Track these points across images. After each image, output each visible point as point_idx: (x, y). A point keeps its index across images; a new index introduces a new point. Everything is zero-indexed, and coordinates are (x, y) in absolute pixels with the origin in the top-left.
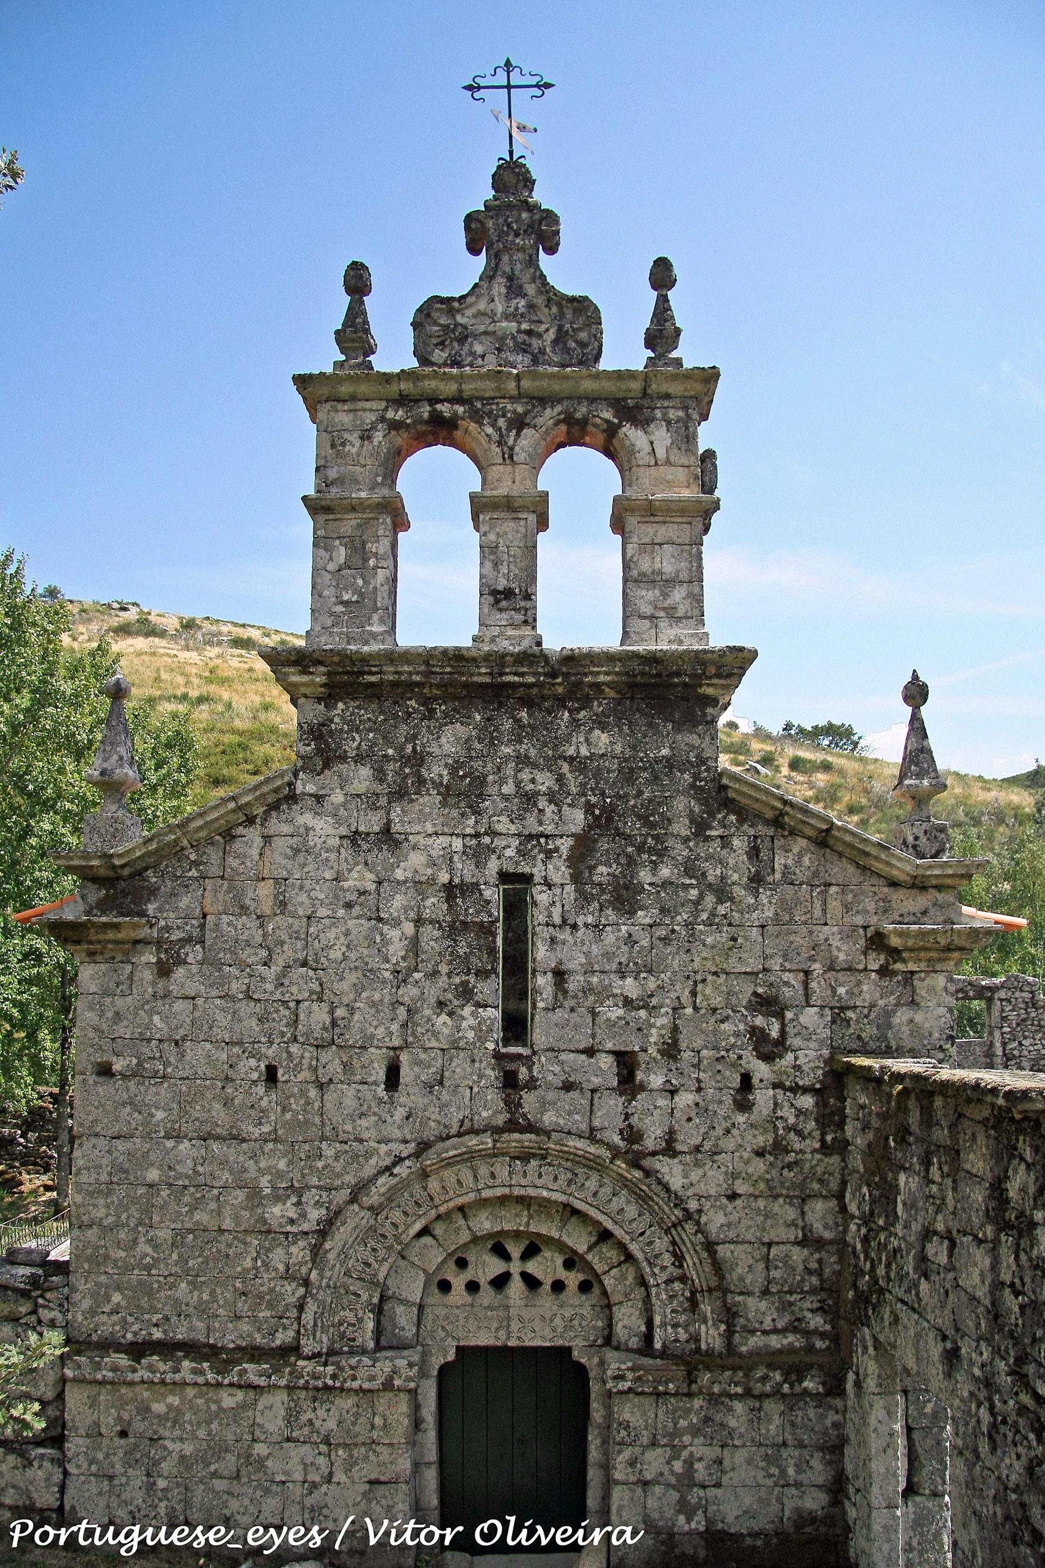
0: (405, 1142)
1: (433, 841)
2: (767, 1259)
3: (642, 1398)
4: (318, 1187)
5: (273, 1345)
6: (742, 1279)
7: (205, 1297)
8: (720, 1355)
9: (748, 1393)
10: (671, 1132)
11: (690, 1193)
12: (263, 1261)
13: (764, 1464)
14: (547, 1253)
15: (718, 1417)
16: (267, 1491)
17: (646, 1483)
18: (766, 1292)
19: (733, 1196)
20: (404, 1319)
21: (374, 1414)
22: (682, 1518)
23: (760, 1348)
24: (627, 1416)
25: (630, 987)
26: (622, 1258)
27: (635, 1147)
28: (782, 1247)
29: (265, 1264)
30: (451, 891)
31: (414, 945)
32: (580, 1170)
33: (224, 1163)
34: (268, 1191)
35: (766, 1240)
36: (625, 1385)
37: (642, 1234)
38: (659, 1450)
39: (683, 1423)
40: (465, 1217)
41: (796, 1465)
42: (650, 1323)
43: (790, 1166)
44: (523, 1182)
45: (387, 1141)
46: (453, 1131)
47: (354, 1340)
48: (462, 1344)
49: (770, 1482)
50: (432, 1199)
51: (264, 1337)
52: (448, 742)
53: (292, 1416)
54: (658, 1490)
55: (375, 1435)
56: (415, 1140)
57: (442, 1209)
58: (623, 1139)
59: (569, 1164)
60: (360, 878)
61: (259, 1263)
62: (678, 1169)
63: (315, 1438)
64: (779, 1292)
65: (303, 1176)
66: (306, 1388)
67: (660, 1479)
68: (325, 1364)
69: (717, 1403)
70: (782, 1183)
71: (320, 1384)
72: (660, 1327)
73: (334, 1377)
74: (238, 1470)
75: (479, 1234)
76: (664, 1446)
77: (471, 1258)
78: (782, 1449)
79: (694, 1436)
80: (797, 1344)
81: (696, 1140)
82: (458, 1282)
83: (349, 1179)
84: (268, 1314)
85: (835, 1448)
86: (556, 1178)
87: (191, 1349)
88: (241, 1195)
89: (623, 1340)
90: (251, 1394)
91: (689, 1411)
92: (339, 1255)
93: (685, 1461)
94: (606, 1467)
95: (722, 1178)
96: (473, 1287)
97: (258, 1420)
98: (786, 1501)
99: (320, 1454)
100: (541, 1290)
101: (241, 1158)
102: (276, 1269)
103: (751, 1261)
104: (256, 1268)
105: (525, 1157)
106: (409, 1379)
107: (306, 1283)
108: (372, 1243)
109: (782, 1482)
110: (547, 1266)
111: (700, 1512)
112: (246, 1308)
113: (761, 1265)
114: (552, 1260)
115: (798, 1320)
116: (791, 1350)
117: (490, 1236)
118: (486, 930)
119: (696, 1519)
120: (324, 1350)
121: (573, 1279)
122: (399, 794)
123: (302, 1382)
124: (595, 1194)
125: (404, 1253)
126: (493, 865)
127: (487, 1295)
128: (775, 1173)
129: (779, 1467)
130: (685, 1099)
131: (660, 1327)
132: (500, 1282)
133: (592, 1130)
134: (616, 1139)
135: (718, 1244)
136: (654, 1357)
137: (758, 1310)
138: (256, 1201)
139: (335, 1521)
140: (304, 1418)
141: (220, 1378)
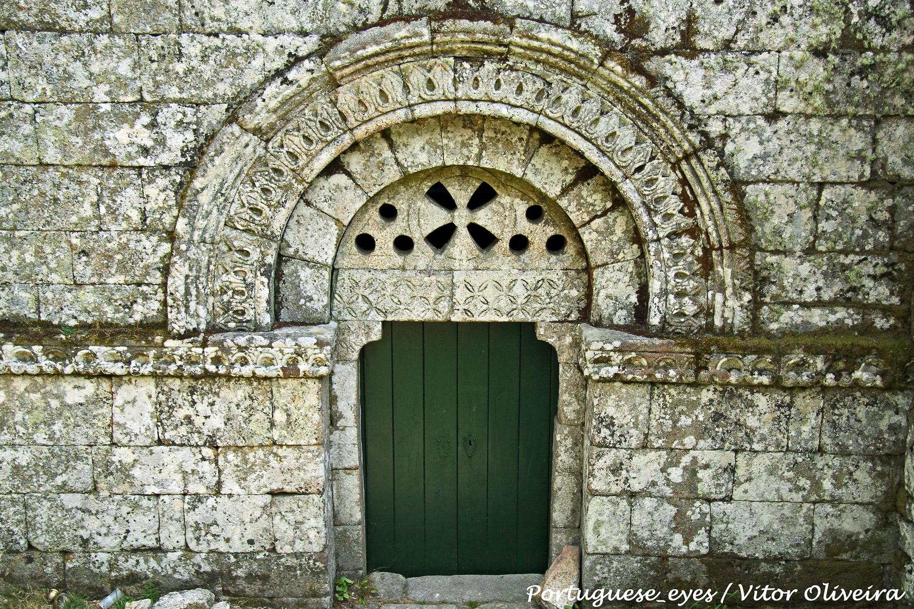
0: (303, 33)
2: (815, 206)
3: (631, 388)
4: (180, 102)
5: (131, 321)
6: (778, 232)
7: (29, 258)
8: (741, 333)
9: (777, 384)
10: (690, 20)
11: (712, 110)
12: (108, 207)
13: (791, 474)
14: (504, 199)
15: (732, 415)
16: (136, 506)
17: (633, 495)
18: (810, 251)
19: (774, 116)
20: (311, 285)
21: (274, 408)
22: (678, 539)
23: (797, 326)
24: (611, 410)
26: (609, 205)
27: (637, 42)
28: (840, 190)
29: (112, 212)
32: (553, 78)
33: (36, 67)
34: (108, 107)
35: (817, 179)
36: (609, 371)
37: (640, 169)
38: (652, 455)
39: (685, 421)
40: (392, 146)
41: (834, 476)
42: (643, 292)
43: (862, 72)
44: (474, 94)
45: (277, 33)
46: (373, 18)
47: (243, 313)
48: (390, 318)
49: (798, 497)
50: (344, 119)
51: (117, 311)
53: (163, 412)
54: (648, 503)
55: (276, 434)
56: (317, 31)
57: (360, 133)
58: (619, 30)
59: (540, 68)
61: (103, 210)
62: (697, 76)
63: (195, 438)
64: (829, 251)
65: (157, 85)
66: (179, 376)
67: (651, 489)
68: (204, 345)
69: (732, 395)
70: (849, 98)
71: (198, 370)
72: (659, 296)
73: (217, 361)
74: (95, 482)
75: (411, 171)
76: (659, 449)
77: (400, 205)
78: (817, 457)
79: (699, 437)
80: (849, 322)
81: (726, 33)
82: (385, 236)
83: (224, 88)
84: (121, 279)
85: (890, 458)
86: (520, 89)
88: (67, 113)
89: (606, 314)
90: (105, 385)
91: (693, 405)
92: (215, 198)
93: (685, 468)
94: (578, 475)
95: (759, 89)
96: (404, 244)
97: (117, 419)
98: (817, 521)
99: (203, 459)
100: (495, 248)
101: (62, 59)
102: (127, 218)
103: (792, 208)
104: (99, 218)
105: (477, 59)
106: (319, 363)
107: (171, 236)
108: (262, 181)
109: (814, 497)
110: (504, 216)
111: (702, 531)
112: (89, 271)
113: (807, 214)
114: (512, 208)
115: (853, 289)
116: (839, 329)
117: (426, 173)
119: (696, 539)
120: (203, 327)
121: (539, 234)
123: (173, 368)
124: (576, 112)
125: (309, 197)
127: (423, 254)
128: (838, 81)
129: (811, 478)
131: (659, 296)
132: (440, 238)
133: (575, 16)
134: (609, 30)
135: (747, 183)
136: (650, 336)
137: (798, 274)
138: (90, 123)
139: (228, 540)
140: (180, 414)
141: (59, 367)
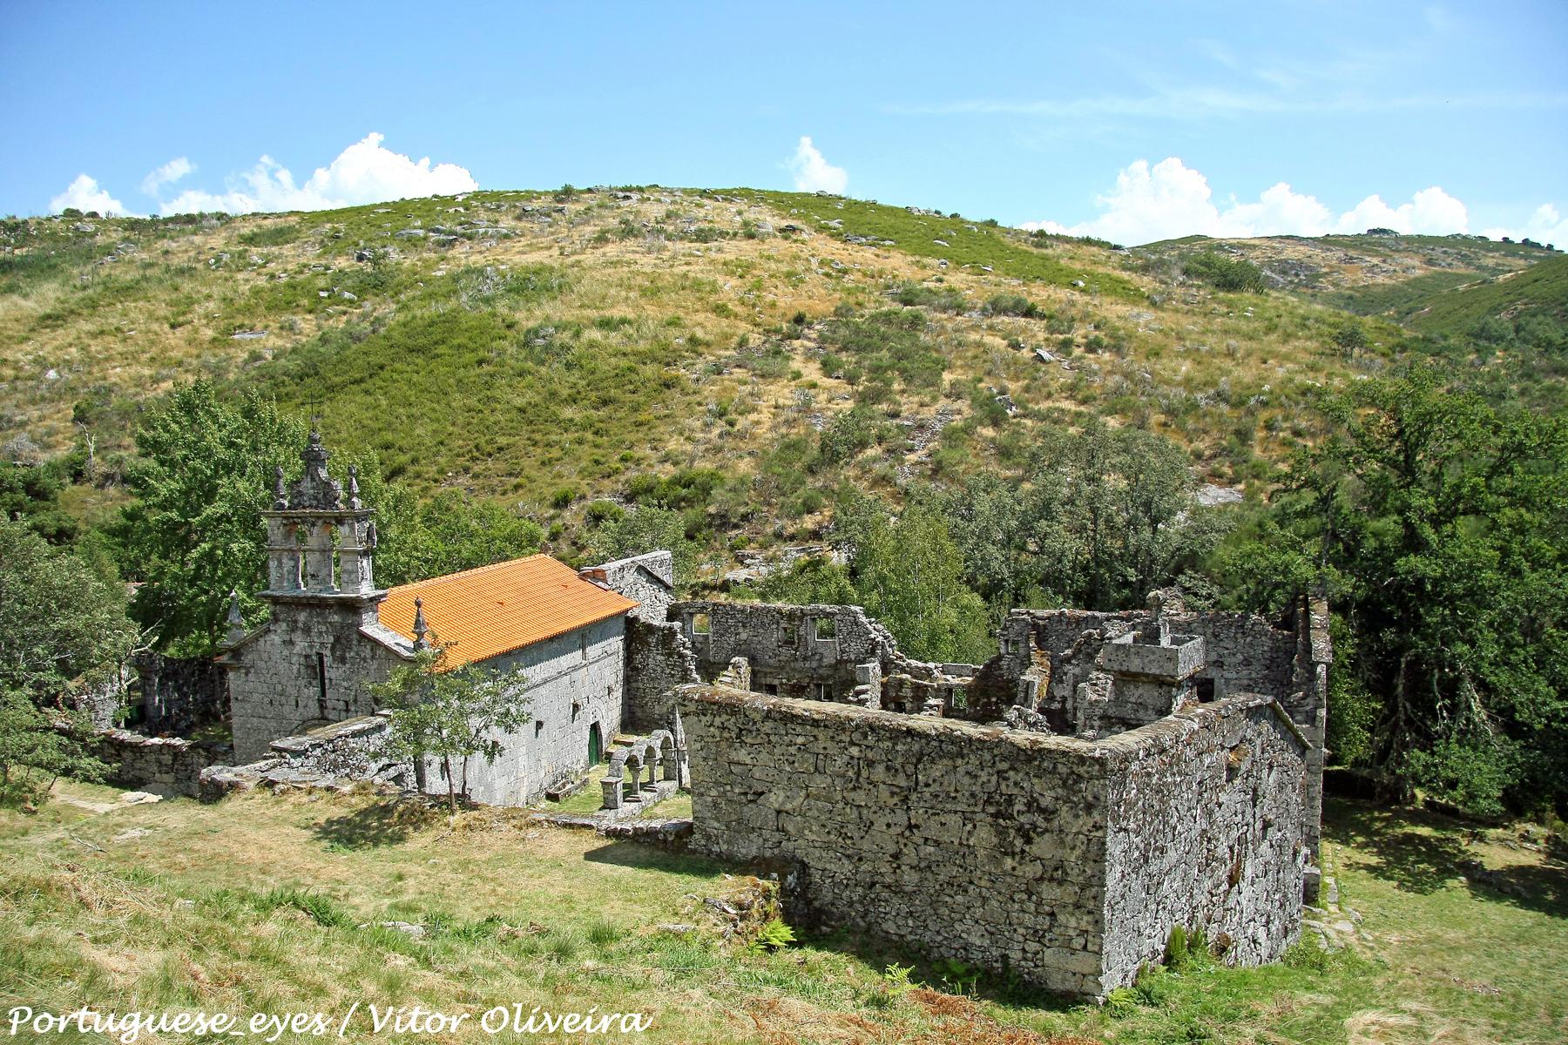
1: (301, 644)
30: (307, 657)
52: (302, 617)
60: (286, 653)
118: (314, 668)
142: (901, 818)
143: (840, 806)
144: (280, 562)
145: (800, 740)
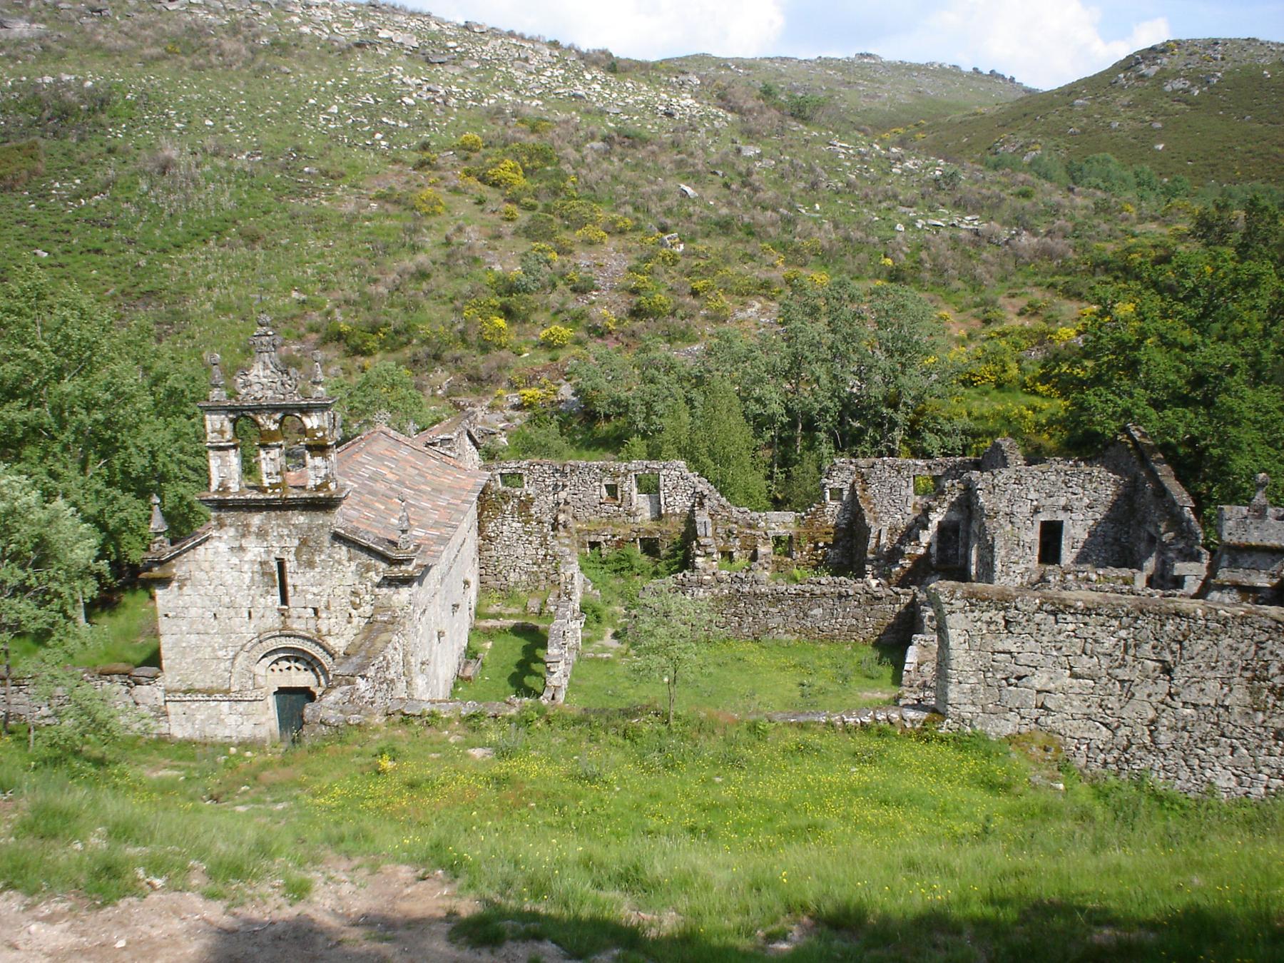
1: (255, 550)
25: (315, 590)
30: (261, 563)
31: (252, 579)
52: (256, 519)
53: (230, 707)
60: (235, 560)
87: (199, 691)
122: (243, 536)
126: (273, 556)
130: (333, 620)
132: (289, 668)
142: (1163, 686)
143: (1104, 680)
144: (224, 464)
145: (1071, 627)
